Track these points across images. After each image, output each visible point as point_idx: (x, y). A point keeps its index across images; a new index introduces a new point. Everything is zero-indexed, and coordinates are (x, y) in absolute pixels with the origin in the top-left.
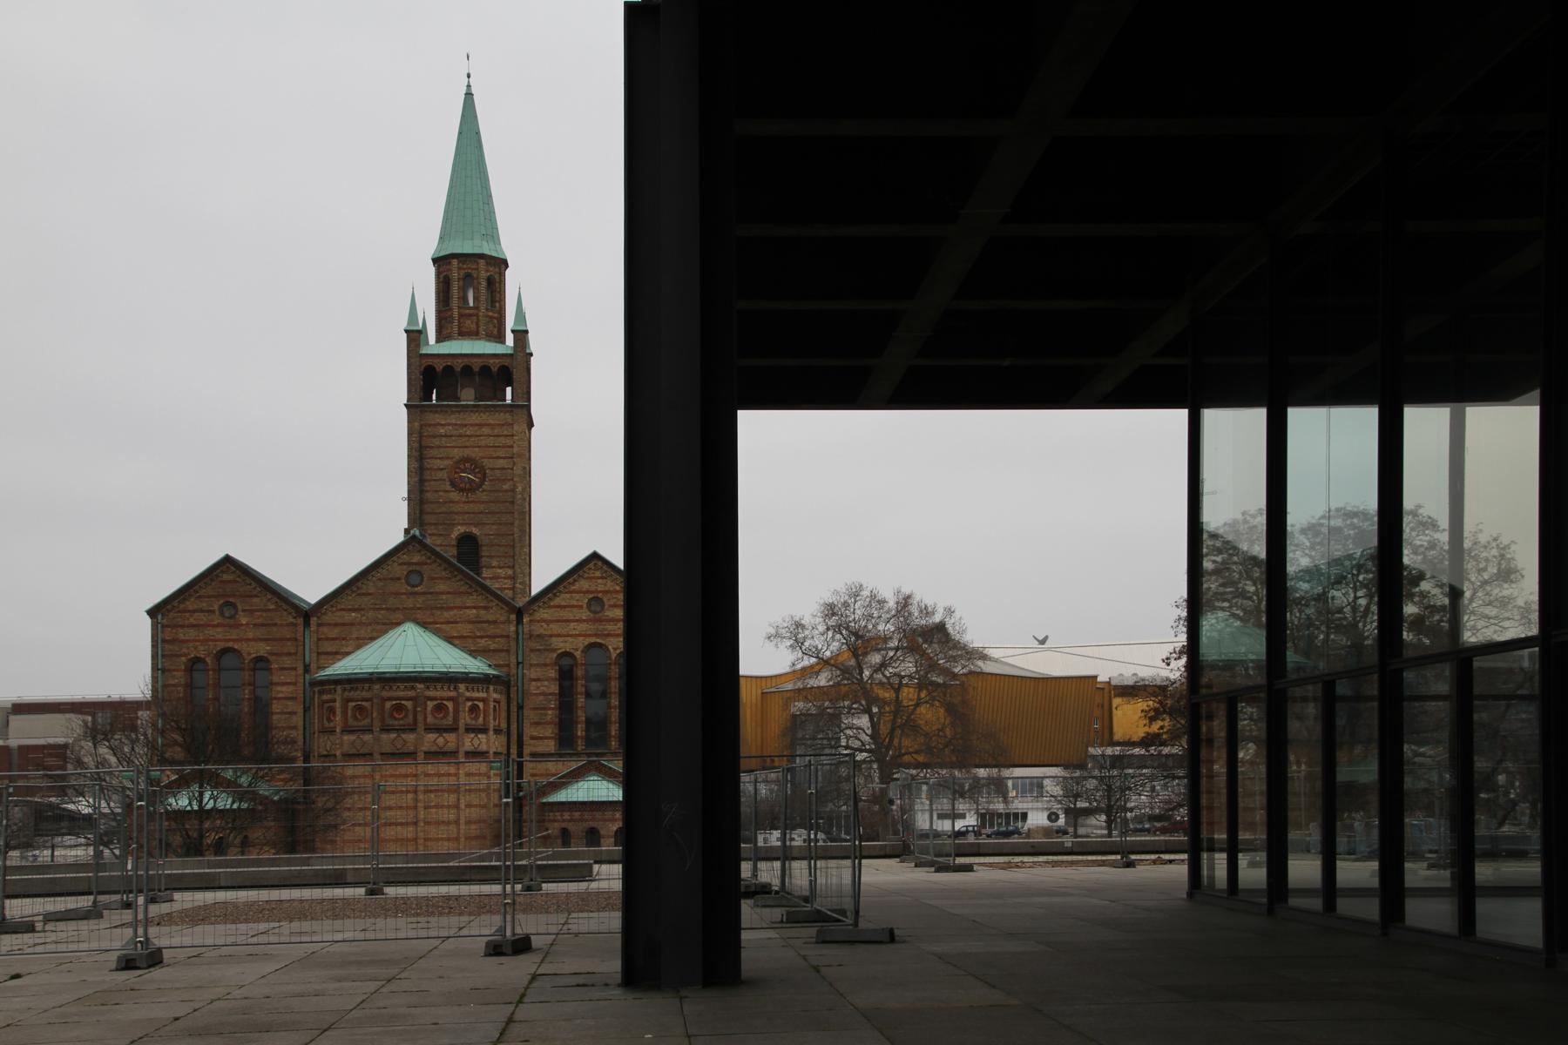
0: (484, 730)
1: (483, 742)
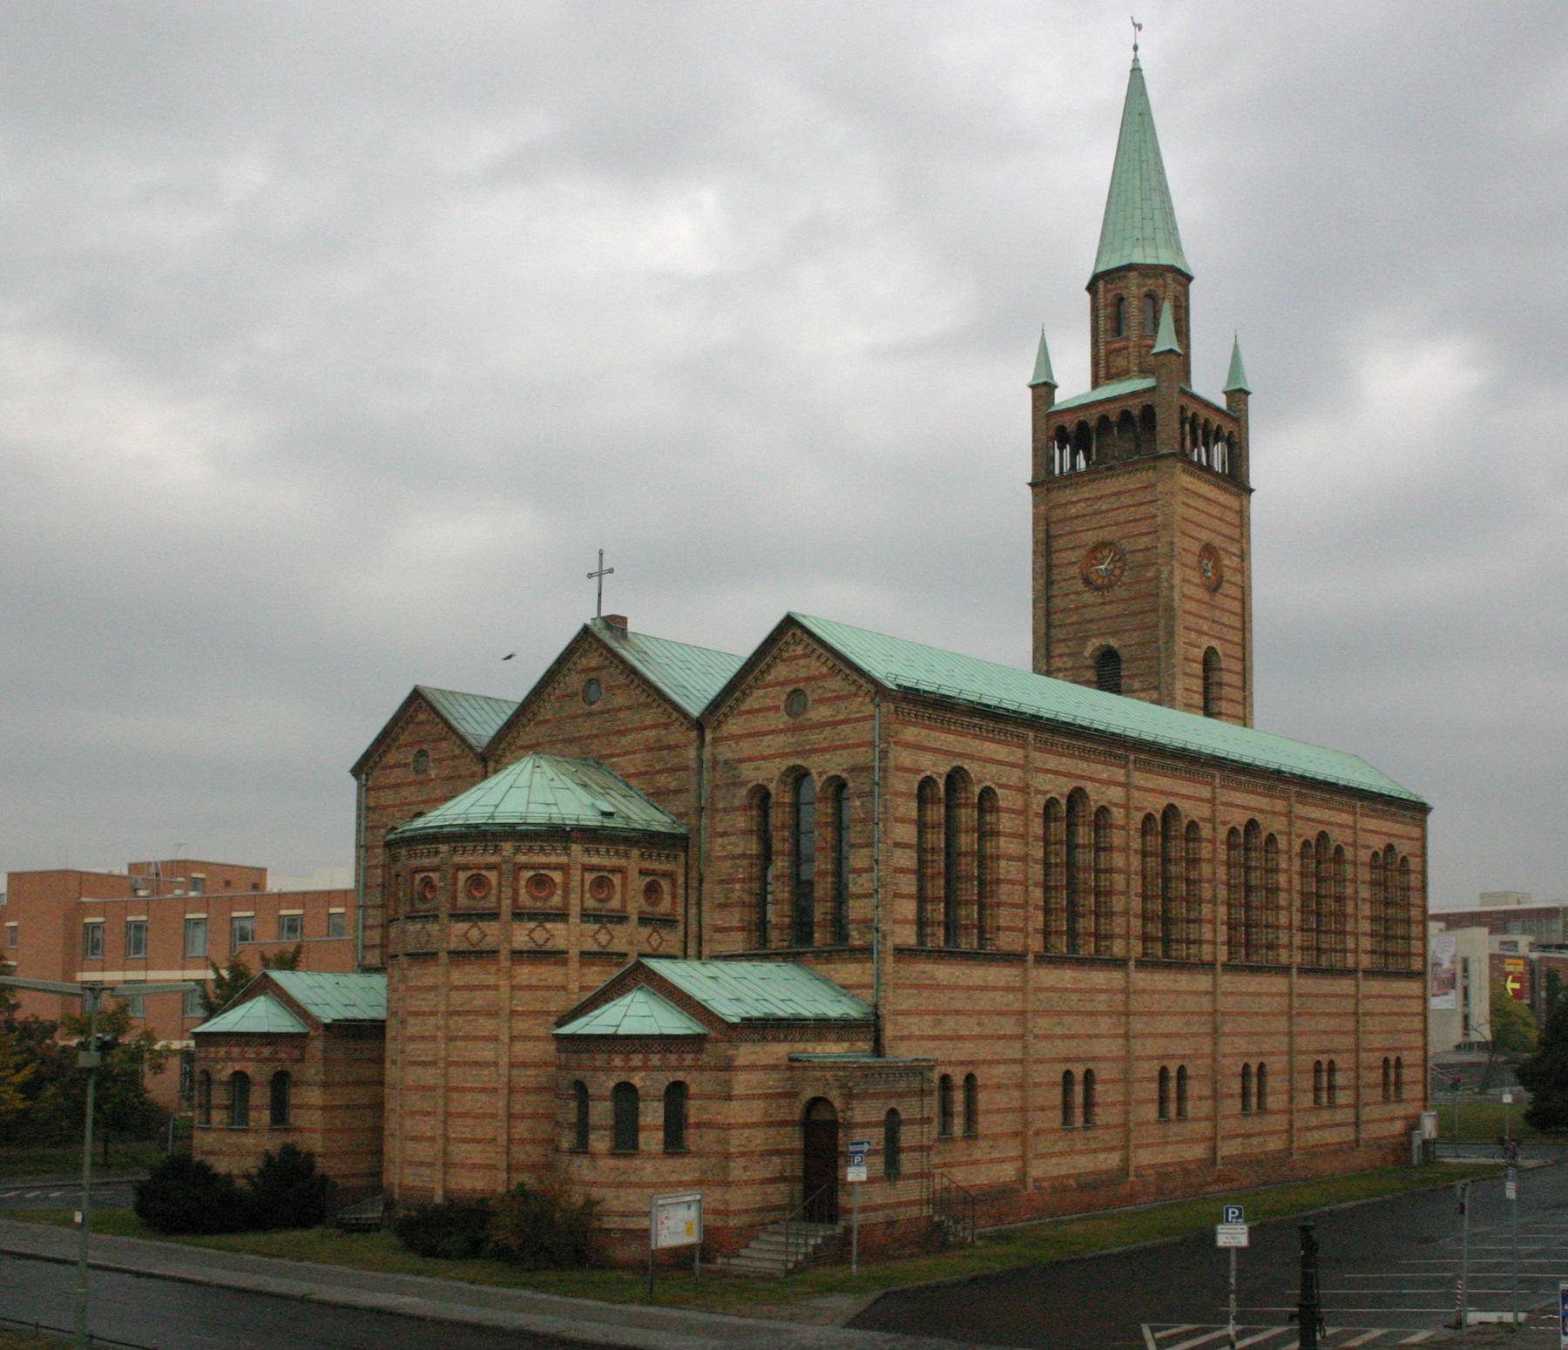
0: (561, 916)
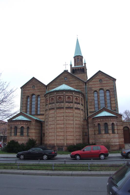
0: (79, 104)
1: (79, 106)
